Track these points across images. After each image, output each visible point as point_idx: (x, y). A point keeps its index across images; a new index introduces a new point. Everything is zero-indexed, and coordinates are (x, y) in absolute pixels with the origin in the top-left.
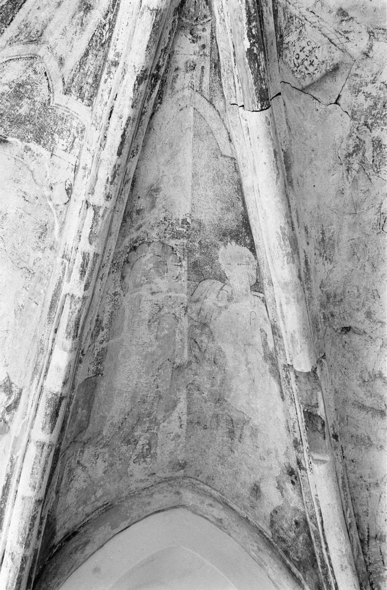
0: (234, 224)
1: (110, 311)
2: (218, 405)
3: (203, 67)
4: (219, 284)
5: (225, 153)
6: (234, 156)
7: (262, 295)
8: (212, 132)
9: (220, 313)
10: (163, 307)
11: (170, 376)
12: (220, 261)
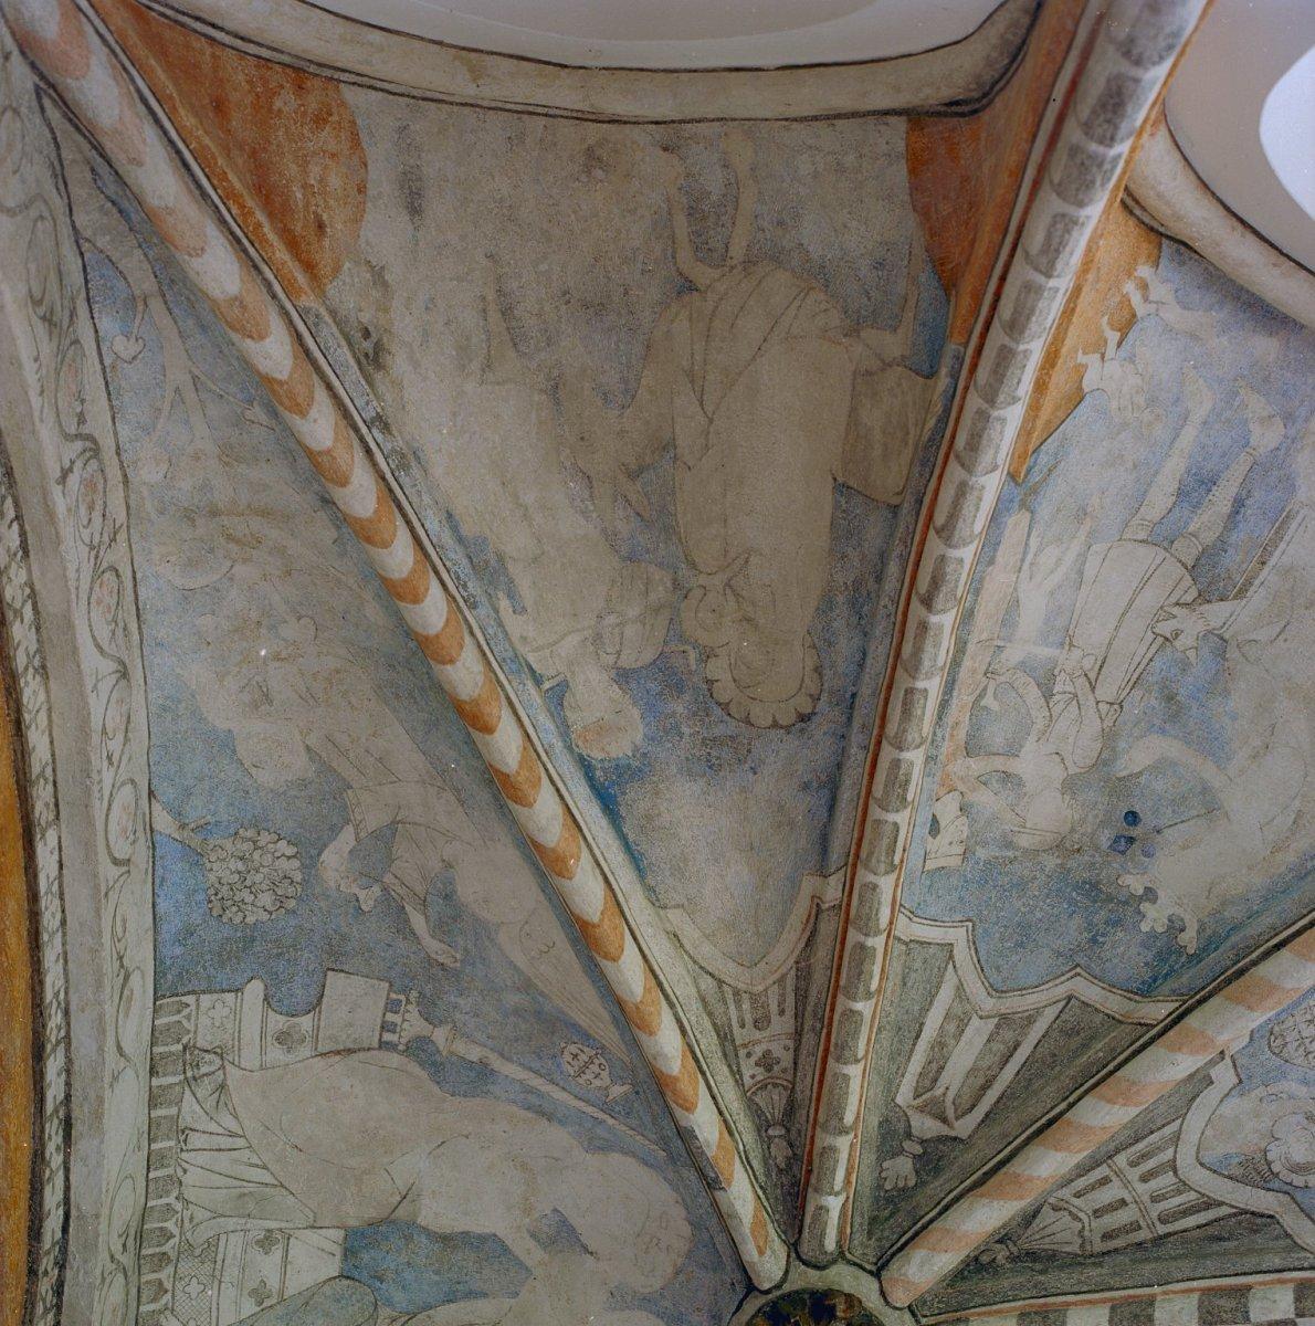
0: (631, 795)
1: (834, 615)
2: (556, 372)
3: (743, 1026)
4: (628, 660)
5: (678, 912)
6: (662, 912)
7: (547, 685)
8: (707, 937)
9: (608, 600)
10: (724, 590)
11: (678, 428)
12: (636, 713)
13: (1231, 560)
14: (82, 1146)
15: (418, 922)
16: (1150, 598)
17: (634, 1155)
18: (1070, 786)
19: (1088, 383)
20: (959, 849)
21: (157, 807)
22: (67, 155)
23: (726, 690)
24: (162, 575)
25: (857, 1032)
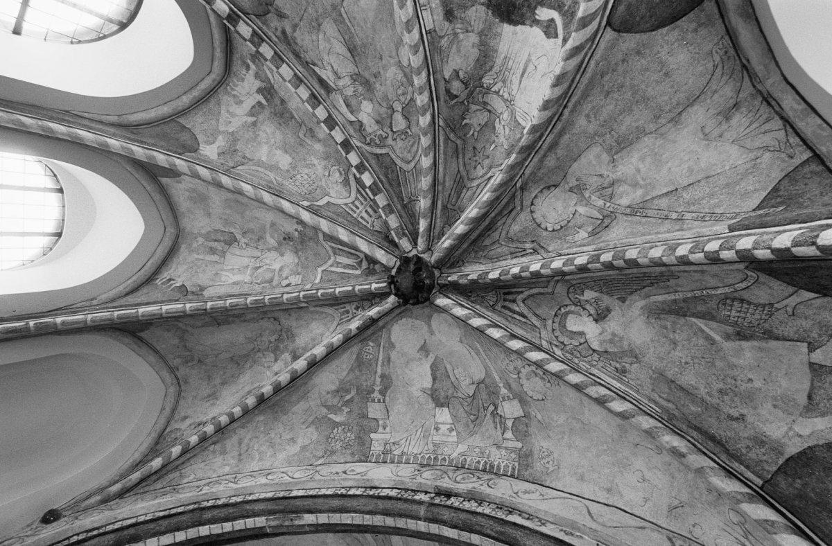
13: (226, 238)
14: (377, 484)
15: (348, 397)
16: (238, 252)
17: (389, 337)
18: (282, 255)
19: (178, 285)
20: (298, 276)
21: (316, 463)
22: (142, 491)
23: (276, 336)
24: (254, 465)
25: (326, 293)
